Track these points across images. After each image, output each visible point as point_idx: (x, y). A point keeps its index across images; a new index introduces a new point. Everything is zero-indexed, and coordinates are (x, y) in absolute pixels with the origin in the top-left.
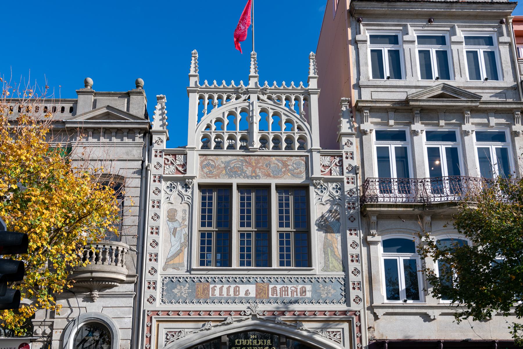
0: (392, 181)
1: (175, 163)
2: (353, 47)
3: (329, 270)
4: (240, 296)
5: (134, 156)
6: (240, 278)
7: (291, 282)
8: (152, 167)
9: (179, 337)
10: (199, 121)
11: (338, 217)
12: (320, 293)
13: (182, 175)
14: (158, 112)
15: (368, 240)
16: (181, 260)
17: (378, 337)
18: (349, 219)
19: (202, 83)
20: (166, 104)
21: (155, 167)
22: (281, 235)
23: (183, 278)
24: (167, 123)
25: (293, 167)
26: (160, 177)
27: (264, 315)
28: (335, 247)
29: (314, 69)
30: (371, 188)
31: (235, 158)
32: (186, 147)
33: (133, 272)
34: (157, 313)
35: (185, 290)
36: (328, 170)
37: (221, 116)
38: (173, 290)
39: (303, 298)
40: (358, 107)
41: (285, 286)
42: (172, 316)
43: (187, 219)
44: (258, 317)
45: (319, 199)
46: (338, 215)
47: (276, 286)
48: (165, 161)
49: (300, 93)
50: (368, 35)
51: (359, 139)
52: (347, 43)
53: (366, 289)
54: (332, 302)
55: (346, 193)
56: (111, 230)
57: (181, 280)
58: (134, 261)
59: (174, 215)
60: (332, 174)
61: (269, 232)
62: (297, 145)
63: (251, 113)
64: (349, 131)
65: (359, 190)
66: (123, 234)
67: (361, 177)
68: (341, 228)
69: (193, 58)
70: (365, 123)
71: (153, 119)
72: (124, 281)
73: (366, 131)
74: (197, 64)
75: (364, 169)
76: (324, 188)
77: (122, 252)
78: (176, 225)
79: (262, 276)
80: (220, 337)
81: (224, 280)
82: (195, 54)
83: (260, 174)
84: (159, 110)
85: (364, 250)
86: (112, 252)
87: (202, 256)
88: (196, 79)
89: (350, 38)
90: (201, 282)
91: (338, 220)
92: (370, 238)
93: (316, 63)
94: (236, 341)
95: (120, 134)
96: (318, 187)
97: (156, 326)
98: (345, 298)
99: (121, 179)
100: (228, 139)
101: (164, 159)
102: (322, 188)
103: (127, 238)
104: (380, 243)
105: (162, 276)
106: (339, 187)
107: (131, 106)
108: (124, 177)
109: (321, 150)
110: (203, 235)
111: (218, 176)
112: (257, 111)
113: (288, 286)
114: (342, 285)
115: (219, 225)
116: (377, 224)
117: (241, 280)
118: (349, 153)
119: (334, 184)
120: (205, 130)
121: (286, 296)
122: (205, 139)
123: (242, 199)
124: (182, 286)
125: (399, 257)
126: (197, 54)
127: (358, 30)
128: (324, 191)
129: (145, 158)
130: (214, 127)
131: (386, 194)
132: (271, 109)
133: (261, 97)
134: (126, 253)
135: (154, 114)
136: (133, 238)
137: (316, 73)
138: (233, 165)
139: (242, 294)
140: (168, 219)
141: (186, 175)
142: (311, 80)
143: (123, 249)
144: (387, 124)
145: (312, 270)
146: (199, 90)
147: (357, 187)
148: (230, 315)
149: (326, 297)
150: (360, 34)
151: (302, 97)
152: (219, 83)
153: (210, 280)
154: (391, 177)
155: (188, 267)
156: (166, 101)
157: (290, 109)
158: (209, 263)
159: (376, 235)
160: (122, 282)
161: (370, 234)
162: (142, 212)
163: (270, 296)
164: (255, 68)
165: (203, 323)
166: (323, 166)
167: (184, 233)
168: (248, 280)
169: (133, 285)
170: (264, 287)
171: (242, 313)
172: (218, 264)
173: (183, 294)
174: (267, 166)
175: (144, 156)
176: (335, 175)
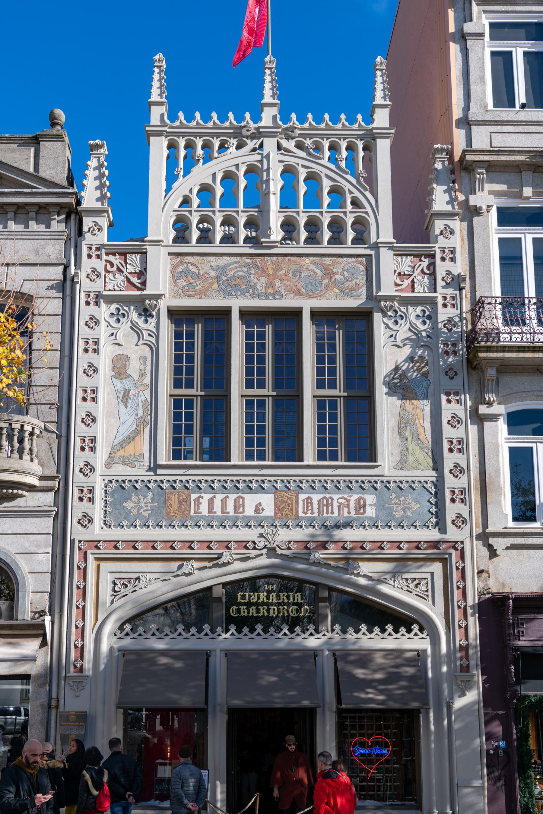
0: (527, 302)
1: (124, 270)
2: (458, 46)
3: (408, 467)
4: (246, 514)
5: (50, 256)
6: (245, 481)
7: (339, 489)
8: (82, 277)
9: (136, 588)
10: (168, 189)
11: (425, 369)
12: (391, 510)
13: (139, 293)
14: (91, 174)
15: (481, 412)
17: (495, 588)
18: (446, 373)
19: (173, 117)
20: (107, 158)
21: (88, 277)
22: (320, 403)
23: (143, 481)
24: (108, 194)
25: (344, 276)
26: (98, 296)
27: (289, 548)
28: (418, 425)
29: (383, 90)
30: (488, 316)
31: (235, 259)
32: (146, 239)
33: (52, 471)
34: (96, 544)
35: (145, 503)
36: (407, 282)
37: (210, 181)
38: (125, 504)
39: (359, 518)
40: (465, 162)
41: (328, 496)
42: (124, 551)
43: (149, 375)
44: (279, 552)
45: (392, 336)
46: (425, 365)
47: (312, 496)
48: (106, 266)
49: (358, 137)
50: (486, 23)
51: (465, 224)
52: (448, 38)
53: (475, 502)
54: (412, 525)
55: (440, 326)
56: (11, 394)
57: (139, 485)
58: (54, 451)
59: (125, 367)
60: (416, 290)
61: (298, 397)
62: (351, 235)
63: (265, 174)
64: (449, 208)
65: (466, 319)
66: (32, 401)
67: (469, 296)
68: (431, 390)
69: (156, 70)
70: (479, 194)
71: (82, 187)
72: (35, 486)
73: (481, 208)
74: (163, 81)
75: (475, 281)
76: (400, 316)
78: (127, 384)
79: (285, 479)
80: (210, 589)
81: (216, 485)
82: (159, 61)
83: (282, 290)
84: (95, 169)
85: (473, 430)
86: (13, 435)
87: (177, 442)
88: (163, 109)
89: (452, 29)
90: (175, 489)
91: (426, 375)
92: (483, 409)
93: (387, 77)
94: (239, 597)
95: (23, 216)
96: (390, 313)
97: (94, 567)
98: (437, 517)
99: (27, 300)
100: (223, 224)
101: (104, 263)
102: (396, 316)
103: (39, 408)
104: (502, 418)
105: (104, 477)
106: (427, 313)
107: (41, 162)
108: (32, 296)
109: (395, 245)
110: (177, 403)
111: (204, 293)
112: (276, 171)
113: (332, 496)
114: (431, 493)
115: (206, 385)
116: (498, 383)
117: (248, 486)
118: (447, 251)
119: (419, 309)
120: (179, 207)
121: (330, 515)
122: (179, 225)
123: (249, 336)
124: (140, 497)
125: (536, 443)
126: (164, 62)
127: (467, 13)
128: (400, 322)
129: (69, 261)
130: (196, 202)
131: (514, 328)
132: (303, 166)
133: (285, 143)
134: (38, 436)
135: (85, 176)
136: (50, 408)
137: (387, 98)
138: (232, 273)
139: (250, 511)
140: (113, 373)
141: (145, 292)
142: (377, 110)
144: (519, 195)
145: (377, 466)
146: (168, 130)
147: (461, 314)
148: (228, 548)
149: (402, 516)
150: (471, 20)
151: (360, 144)
152: (206, 118)
153: (191, 485)
154: (524, 295)
155: (150, 462)
156: (107, 153)
157: (339, 167)
158: (188, 455)
159: (496, 403)
160: (31, 488)
161: (484, 402)
162: (66, 360)
163: (301, 514)
164: (272, 89)
165: (180, 563)
167: (143, 399)
168: (260, 486)
169: (51, 495)
170: (289, 498)
171: (251, 546)
172: (206, 456)
173: (142, 511)
174: (294, 275)
175: (67, 256)
176: (421, 291)
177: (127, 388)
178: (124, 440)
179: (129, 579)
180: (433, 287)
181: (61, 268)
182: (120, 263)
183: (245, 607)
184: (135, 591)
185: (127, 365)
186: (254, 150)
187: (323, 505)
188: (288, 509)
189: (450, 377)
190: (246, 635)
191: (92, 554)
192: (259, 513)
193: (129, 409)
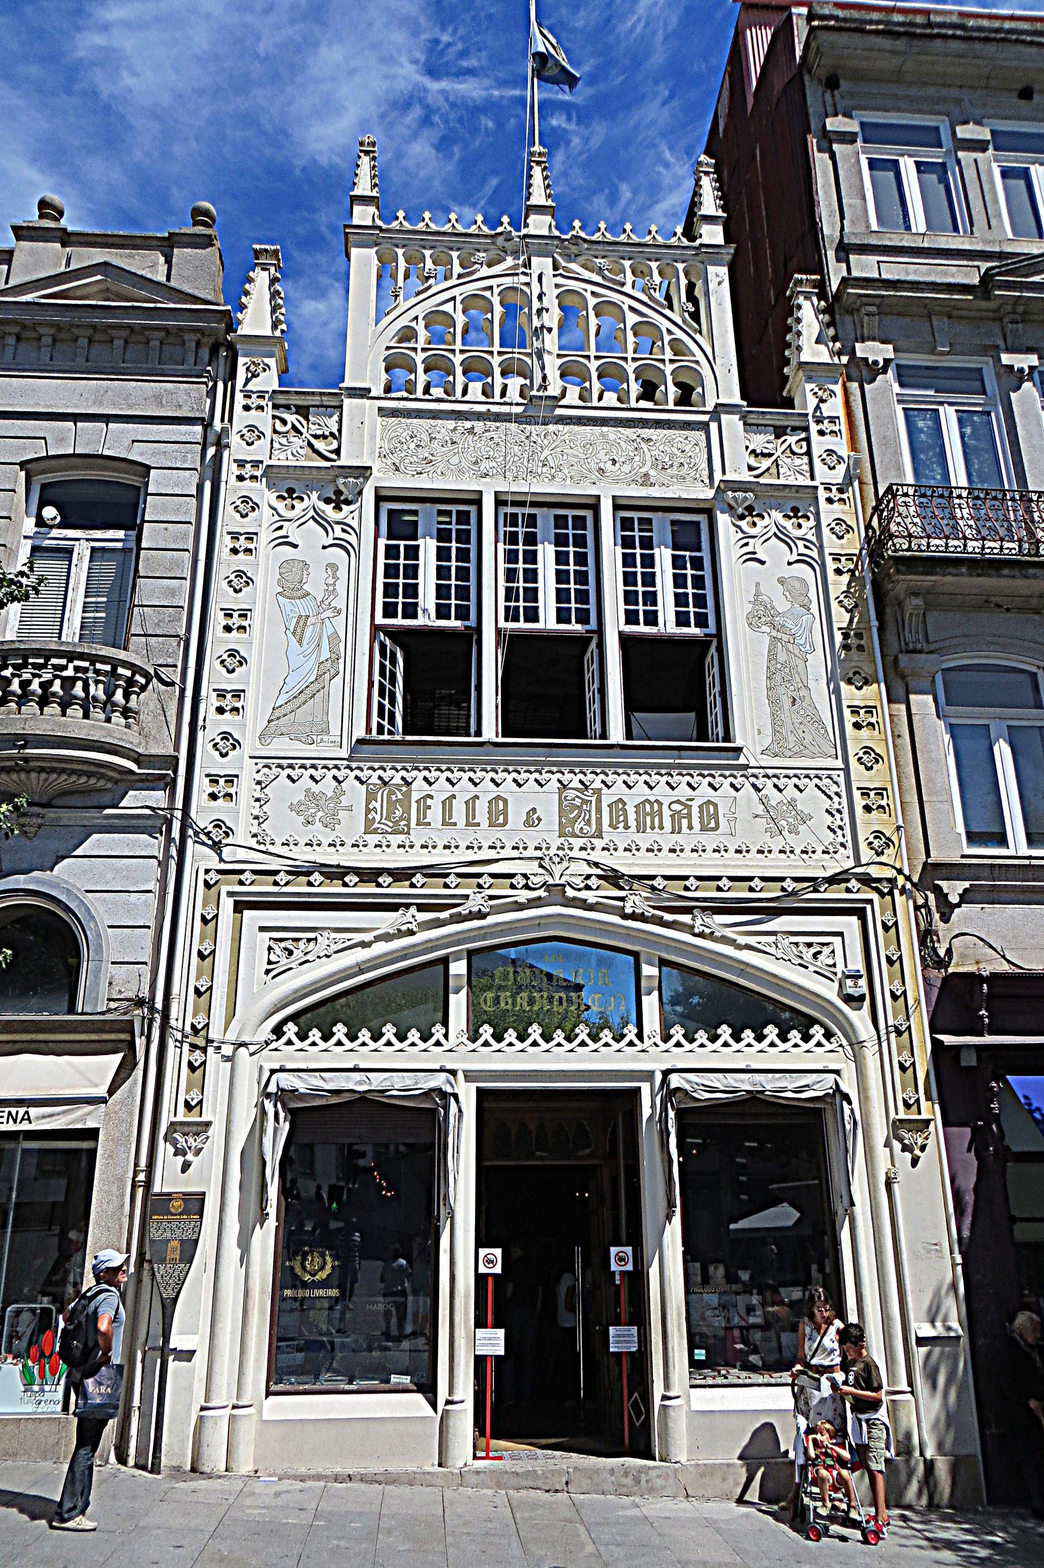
8: (234, 439)
9: (308, 957)
13: (328, 464)
16: (319, 713)
27: (588, 888)
44: (570, 893)
77: (130, 682)
78: (303, 607)
80: (445, 961)
113: (660, 799)
130: (423, 334)
141: (338, 463)
143: (133, 675)
167: (331, 631)
179: (298, 940)
183: (508, 994)
184: (307, 961)
190: (511, 1044)
191: (230, 894)
193: (305, 646)
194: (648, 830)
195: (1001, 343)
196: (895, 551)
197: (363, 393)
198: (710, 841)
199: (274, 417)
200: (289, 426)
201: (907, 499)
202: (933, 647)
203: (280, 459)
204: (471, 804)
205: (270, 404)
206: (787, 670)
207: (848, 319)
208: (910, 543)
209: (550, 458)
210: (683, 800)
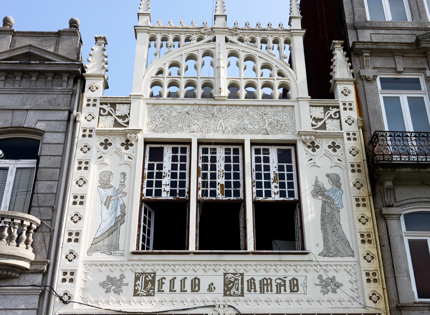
1: (113, 114)
8: (81, 118)
15: (383, 213)
36: (320, 124)
48: (100, 111)
60: (327, 129)
78: (109, 192)
113: (271, 277)
133: (230, 38)
140: (100, 185)
145: (306, 254)
166: (314, 118)
167: (121, 203)
170: (236, 279)
177: (109, 195)
178: (104, 233)
180: (340, 127)
181: (66, 113)
182: (111, 110)
185: (111, 178)
186: (209, 41)
187: (264, 285)
188: (235, 288)
189: (357, 188)
192: (211, 291)
193: (110, 210)
194: (265, 292)
195: (427, 67)
196: (377, 161)
197: (139, 97)
198: (294, 296)
199: (101, 108)
200: (107, 113)
201: (383, 138)
202: (398, 204)
203: (101, 127)
204: (183, 282)
205: (99, 104)
206: (330, 216)
207: (357, 59)
208: (384, 157)
209: (222, 123)
210: (282, 278)
